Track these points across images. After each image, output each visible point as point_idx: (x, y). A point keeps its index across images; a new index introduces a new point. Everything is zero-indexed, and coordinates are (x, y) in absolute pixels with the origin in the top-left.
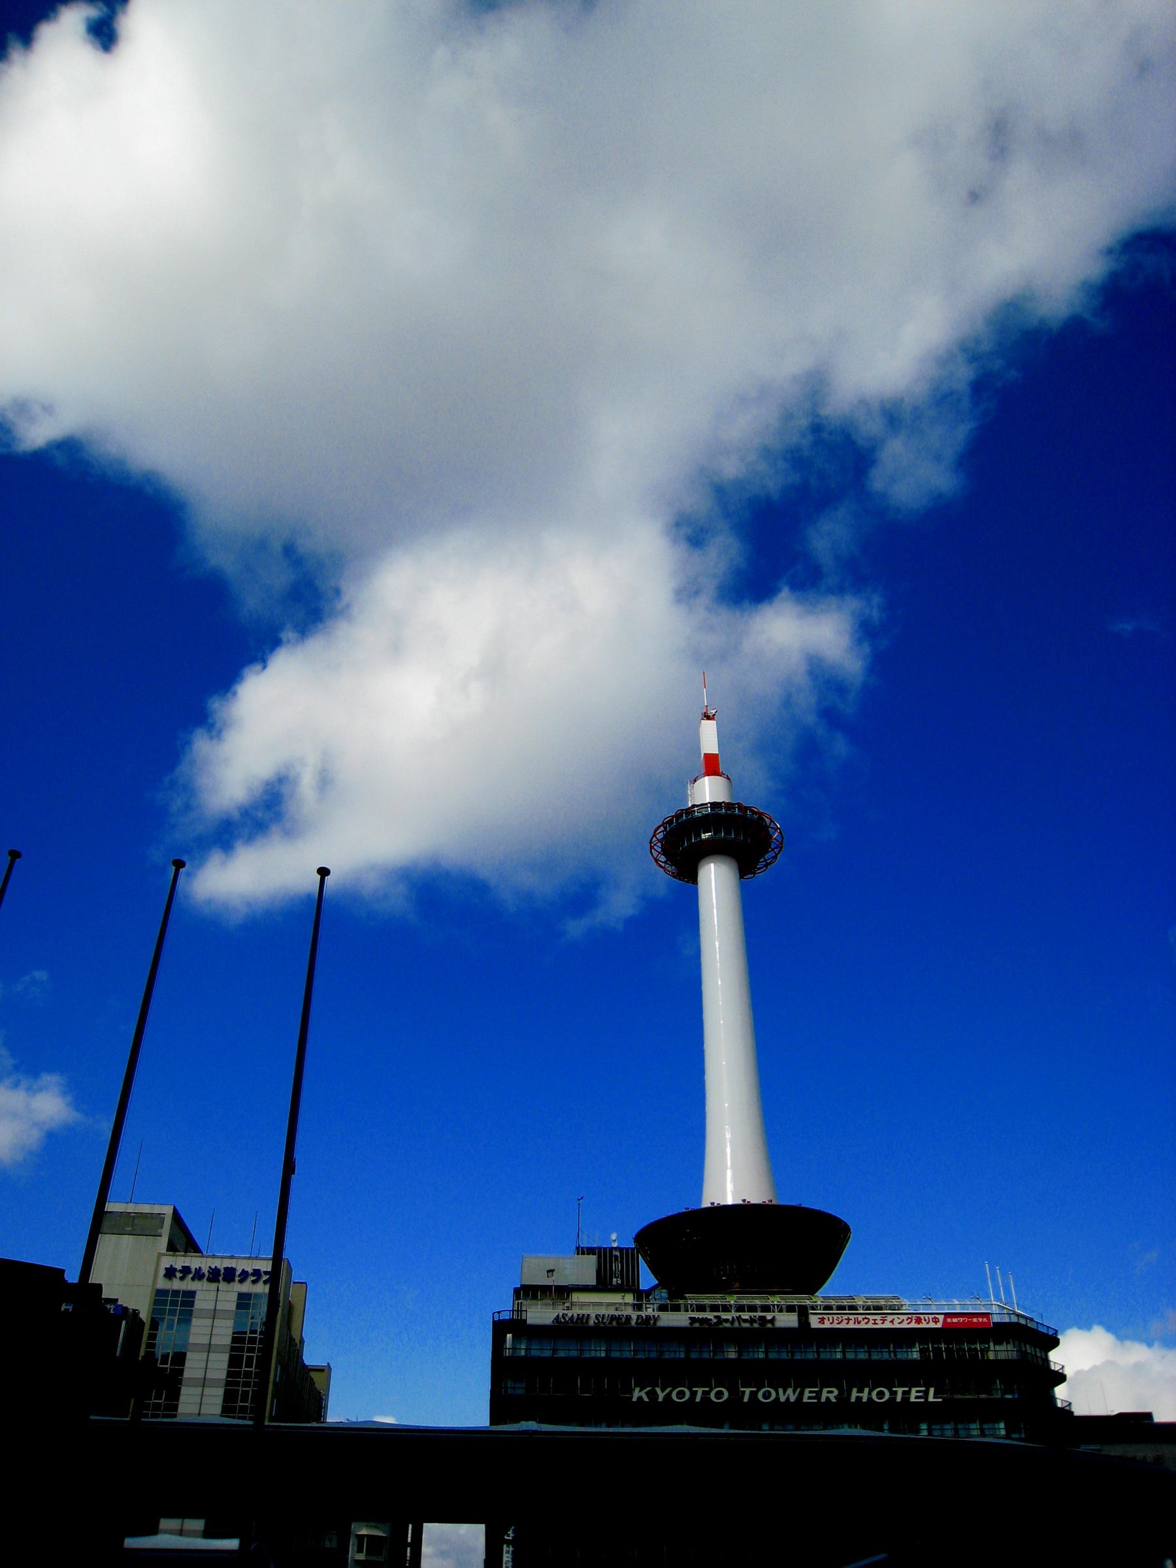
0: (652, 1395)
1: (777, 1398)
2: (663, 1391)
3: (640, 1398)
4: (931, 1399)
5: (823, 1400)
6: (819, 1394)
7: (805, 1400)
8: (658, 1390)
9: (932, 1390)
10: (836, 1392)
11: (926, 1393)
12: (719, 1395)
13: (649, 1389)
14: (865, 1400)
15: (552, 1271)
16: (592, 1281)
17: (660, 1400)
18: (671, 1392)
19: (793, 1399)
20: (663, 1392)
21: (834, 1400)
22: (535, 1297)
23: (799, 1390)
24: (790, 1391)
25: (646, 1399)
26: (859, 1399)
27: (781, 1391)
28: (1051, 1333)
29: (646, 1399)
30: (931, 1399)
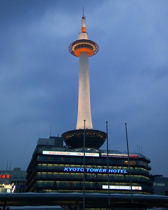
0: (69, 169)
2: (71, 168)
4: (125, 172)
7: (100, 171)
9: (125, 170)
11: (124, 171)
15: (48, 143)
18: (72, 169)
20: (71, 168)
22: (41, 148)
24: (97, 169)
25: (67, 170)
26: (111, 171)
29: (67, 170)
30: (125, 172)
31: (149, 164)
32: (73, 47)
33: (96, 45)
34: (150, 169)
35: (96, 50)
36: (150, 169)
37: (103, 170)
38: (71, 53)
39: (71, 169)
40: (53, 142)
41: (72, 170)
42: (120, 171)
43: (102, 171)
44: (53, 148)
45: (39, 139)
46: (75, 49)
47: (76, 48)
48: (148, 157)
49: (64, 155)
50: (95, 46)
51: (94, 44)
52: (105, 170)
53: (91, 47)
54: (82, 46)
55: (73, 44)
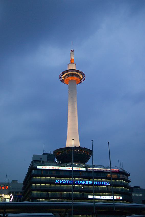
1: (81, 183)
2: (61, 181)
3: (57, 182)
5: (89, 183)
7: (86, 183)
9: (108, 183)
10: (91, 182)
11: (107, 183)
14: (96, 184)
15: (41, 158)
16: (46, 160)
20: (61, 181)
22: (36, 163)
24: (83, 181)
25: (58, 182)
26: (95, 183)
27: (82, 181)
28: (129, 173)
29: (58, 182)
30: (108, 184)
31: (129, 177)
32: (63, 76)
33: (83, 74)
34: (129, 181)
35: (83, 79)
36: (129, 181)
37: (89, 182)
38: (61, 81)
39: (62, 181)
40: (45, 158)
41: (62, 182)
42: (104, 183)
43: (88, 183)
44: (46, 163)
45: (34, 155)
46: (65, 77)
47: (66, 77)
48: (128, 171)
49: (55, 169)
50: (82, 75)
51: (81, 73)
52: (90, 183)
53: (79, 75)
54: (71, 75)
55: (63, 73)
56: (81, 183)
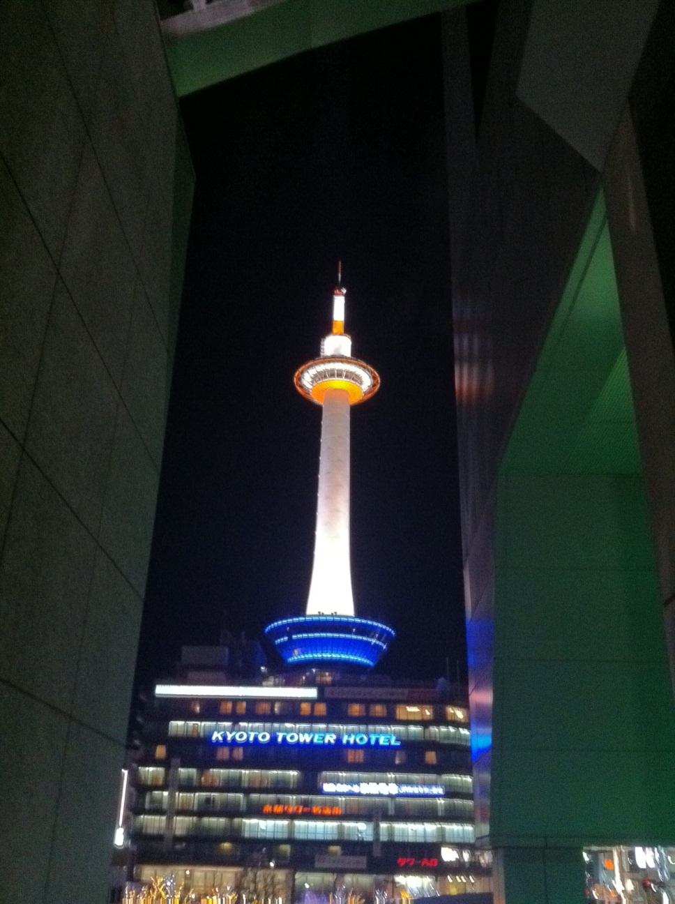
1: (299, 740)
2: (231, 733)
3: (217, 738)
6: (323, 739)
8: (228, 733)
12: (264, 737)
13: (222, 733)
17: (229, 738)
18: (234, 736)
19: (308, 740)
20: (231, 733)
21: (332, 742)
23: (312, 735)
25: (221, 739)
26: (348, 742)
29: (221, 739)
39: (233, 734)
44: (191, 675)
56: (299, 740)
